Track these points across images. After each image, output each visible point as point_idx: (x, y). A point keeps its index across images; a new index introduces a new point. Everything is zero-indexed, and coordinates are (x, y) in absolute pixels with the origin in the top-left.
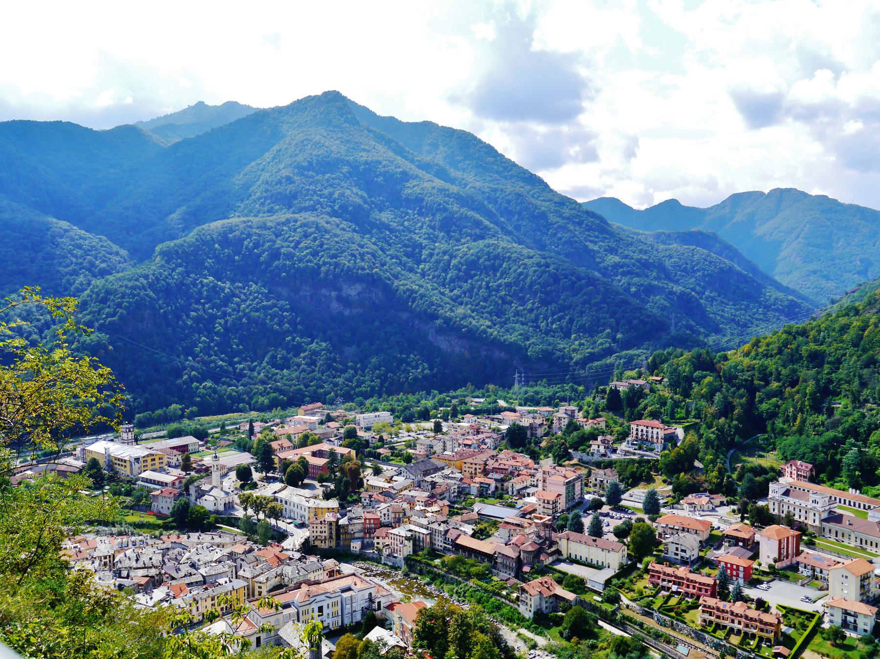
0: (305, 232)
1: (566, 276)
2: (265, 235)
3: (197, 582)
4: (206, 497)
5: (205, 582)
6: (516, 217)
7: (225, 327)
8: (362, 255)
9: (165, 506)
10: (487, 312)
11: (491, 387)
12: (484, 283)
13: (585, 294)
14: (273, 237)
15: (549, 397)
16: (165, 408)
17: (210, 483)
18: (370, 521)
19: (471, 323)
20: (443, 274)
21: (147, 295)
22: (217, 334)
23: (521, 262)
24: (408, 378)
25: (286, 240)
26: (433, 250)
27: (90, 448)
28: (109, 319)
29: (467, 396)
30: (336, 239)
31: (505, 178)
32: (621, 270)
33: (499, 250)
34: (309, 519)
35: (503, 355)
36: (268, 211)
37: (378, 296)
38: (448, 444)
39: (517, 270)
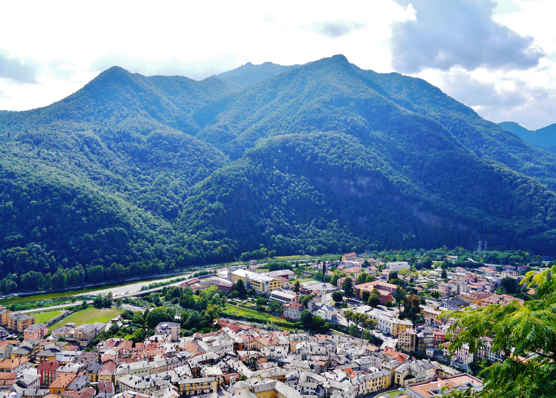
0: (333, 143)
1: (506, 176)
2: (308, 145)
3: (355, 368)
4: (319, 310)
6: (460, 135)
7: (287, 202)
8: (369, 159)
9: (293, 314)
10: (451, 198)
11: (461, 249)
12: (448, 179)
13: (521, 189)
14: (313, 146)
15: (506, 258)
16: (257, 250)
17: (320, 301)
18: (438, 337)
19: (442, 205)
20: (419, 172)
21: (244, 180)
22: (283, 205)
23: (474, 166)
25: (320, 148)
26: (412, 156)
27: (234, 273)
28: (224, 194)
29: (444, 254)
30: (352, 148)
31: (448, 109)
32: (535, 172)
33: (458, 157)
35: (465, 228)
36: (307, 130)
37: (379, 185)
38: (461, 287)
39: (471, 171)
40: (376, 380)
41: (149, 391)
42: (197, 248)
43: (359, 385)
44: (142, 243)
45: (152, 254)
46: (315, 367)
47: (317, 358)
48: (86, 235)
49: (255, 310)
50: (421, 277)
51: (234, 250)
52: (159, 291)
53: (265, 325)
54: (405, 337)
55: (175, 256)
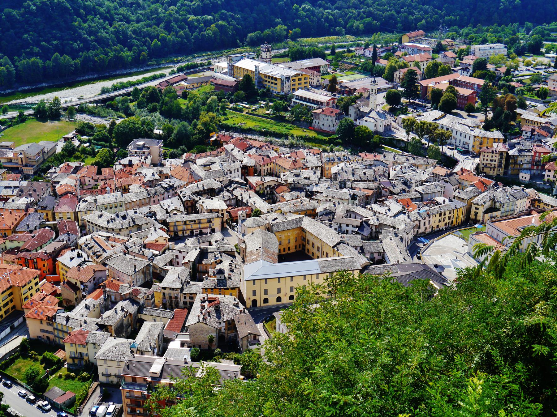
3: (416, 198)
4: (366, 118)
5: (422, 199)
9: (326, 123)
16: (272, 29)
17: (367, 105)
24: (498, 8)
27: (238, 64)
34: (473, 146)
40: (445, 215)
41: (127, 232)
42: (179, 27)
43: (420, 221)
44: (95, 22)
45: (111, 38)
46: (358, 198)
47: (361, 185)
48: (6, 10)
49: (271, 118)
50: (522, 67)
51: (236, 29)
52: (128, 94)
53: (285, 141)
54: (490, 155)
55: (146, 41)
